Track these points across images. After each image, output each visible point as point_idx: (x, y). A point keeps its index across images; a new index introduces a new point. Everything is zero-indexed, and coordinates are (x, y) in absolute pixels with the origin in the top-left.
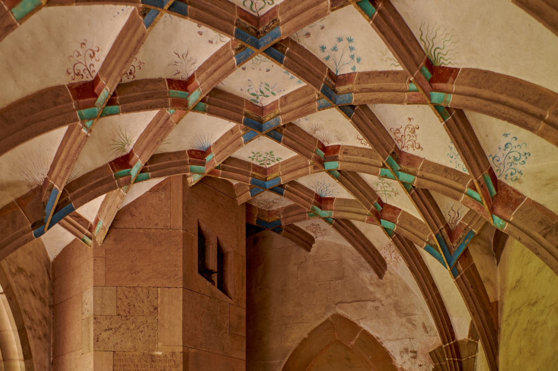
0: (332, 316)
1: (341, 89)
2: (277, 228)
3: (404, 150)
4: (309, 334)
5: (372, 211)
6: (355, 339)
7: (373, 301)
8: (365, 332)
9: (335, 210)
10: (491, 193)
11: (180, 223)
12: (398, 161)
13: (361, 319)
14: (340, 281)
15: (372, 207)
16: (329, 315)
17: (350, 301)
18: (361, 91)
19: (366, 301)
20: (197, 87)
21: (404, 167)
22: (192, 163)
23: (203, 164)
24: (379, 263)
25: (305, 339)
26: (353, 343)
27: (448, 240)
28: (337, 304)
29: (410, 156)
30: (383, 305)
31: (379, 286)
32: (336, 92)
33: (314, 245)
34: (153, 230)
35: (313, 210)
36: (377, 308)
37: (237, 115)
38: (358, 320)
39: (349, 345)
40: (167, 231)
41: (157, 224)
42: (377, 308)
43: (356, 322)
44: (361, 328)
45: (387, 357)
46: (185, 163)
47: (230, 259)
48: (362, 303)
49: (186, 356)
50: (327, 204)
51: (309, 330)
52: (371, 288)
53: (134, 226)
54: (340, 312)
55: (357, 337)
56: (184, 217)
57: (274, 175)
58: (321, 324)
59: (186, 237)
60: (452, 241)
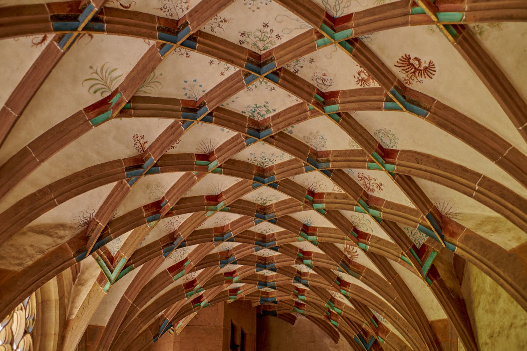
1: (303, 278)
2: (274, 314)
3: (336, 298)
5: (325, 316)
9: (306, 311)
10: (375, 326)
11: (222, 323)
12: (333, 303)
15: (325, 314)
18: (312, 281)
20: (237, 275)
21: (336, 305)
22: (230, 295)
23: (236, 295)
24: (335, 334)
27: (365, 337)
29: (338, 301)
31: (336, 348)
32: (301, 278)
33: (296, 321)
34: (207, 327)
35: (294, 309)
37: (255, 282)
40: (214, 327)
41: (210, 324)
46: (227, 296)
47: (248, 337)
50: (302, 307)
53: (198, 325)
56: (224, 319)
57: (272, 296)
59: (225, 330)
60: (367, 337)
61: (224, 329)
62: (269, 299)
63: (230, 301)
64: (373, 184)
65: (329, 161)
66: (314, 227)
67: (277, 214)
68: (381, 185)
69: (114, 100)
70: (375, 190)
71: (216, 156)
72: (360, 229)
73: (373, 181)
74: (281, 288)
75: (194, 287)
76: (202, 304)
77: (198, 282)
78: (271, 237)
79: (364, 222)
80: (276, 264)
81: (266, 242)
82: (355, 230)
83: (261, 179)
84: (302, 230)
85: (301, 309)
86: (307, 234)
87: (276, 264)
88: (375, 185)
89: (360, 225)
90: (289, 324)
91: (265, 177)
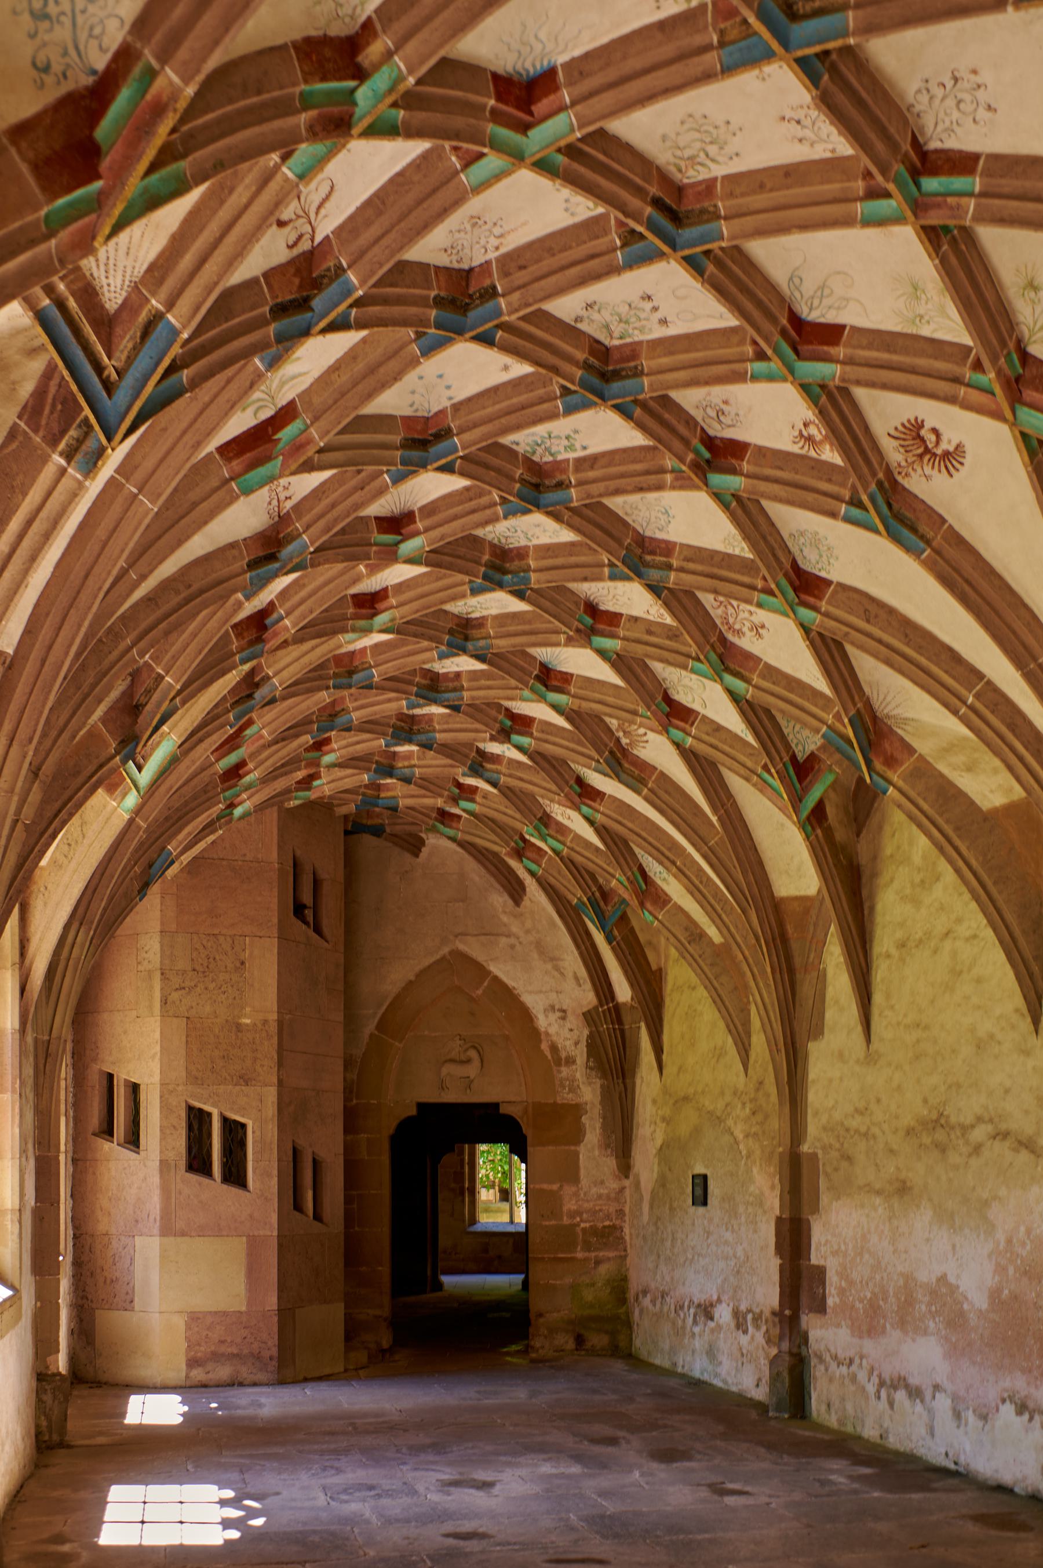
0: (451, 953)
4: (417, 976)
6: (483, 988)
7: (508, 936)
8: (496, 980)
13: (491, 960)
14: (461, 904)
16: (445, 950)
17: (476, 933)
19: (498, 935)
25: (411, 982)
26: (480, 992)
28: (456, 936)
30: (520, 943)
31: (515, 916)
36: (512, 947)
38: (486, 961)
39: (474, 995)
42: (512, 947)
43: (485, 964)
44: (489, 972)
45: (526, 1015)
48: (492, 938)
49: (280, 1023)
51: (417, 969)
52: (505, 919)
53: (215, 856)
54: (462, 947)
55: (486, 984)
58: (434, 963)
61: (279, 870)
62: (380, 801)
63: (293, 804)
64: (745, 622)
65: (669, 567)
66: (566, 673)
67: (495, 642)
68: (763, 627)
69: (287, 434)
70: (744, 634)
71: (420, 525)
72: (676, 697)
73: (746, 615)
74: (428, 784)
75: (241, 777)
76: (238, 812)
77: (251, 766)
78: (452, 680)
79: (690, 684)
80: (437, 735)
81: (437, 691)
82: (668, 699)
83: (497, 576)
84: (538, 678)
85: (451, 827)
86: (546, 686)
87: (437, 735)
88: (748, 624)
89: (680, 689)
90: (408, 857)
91: (505, 572)
